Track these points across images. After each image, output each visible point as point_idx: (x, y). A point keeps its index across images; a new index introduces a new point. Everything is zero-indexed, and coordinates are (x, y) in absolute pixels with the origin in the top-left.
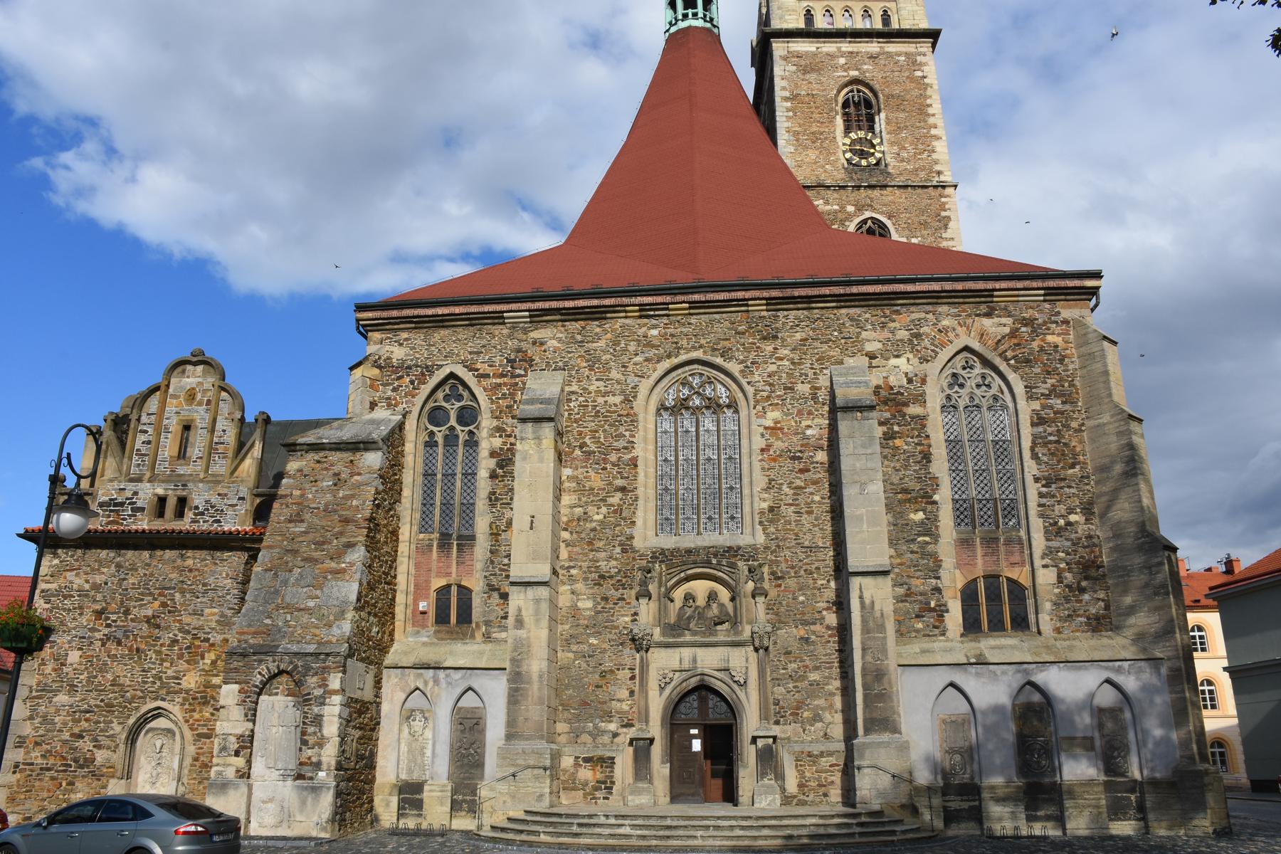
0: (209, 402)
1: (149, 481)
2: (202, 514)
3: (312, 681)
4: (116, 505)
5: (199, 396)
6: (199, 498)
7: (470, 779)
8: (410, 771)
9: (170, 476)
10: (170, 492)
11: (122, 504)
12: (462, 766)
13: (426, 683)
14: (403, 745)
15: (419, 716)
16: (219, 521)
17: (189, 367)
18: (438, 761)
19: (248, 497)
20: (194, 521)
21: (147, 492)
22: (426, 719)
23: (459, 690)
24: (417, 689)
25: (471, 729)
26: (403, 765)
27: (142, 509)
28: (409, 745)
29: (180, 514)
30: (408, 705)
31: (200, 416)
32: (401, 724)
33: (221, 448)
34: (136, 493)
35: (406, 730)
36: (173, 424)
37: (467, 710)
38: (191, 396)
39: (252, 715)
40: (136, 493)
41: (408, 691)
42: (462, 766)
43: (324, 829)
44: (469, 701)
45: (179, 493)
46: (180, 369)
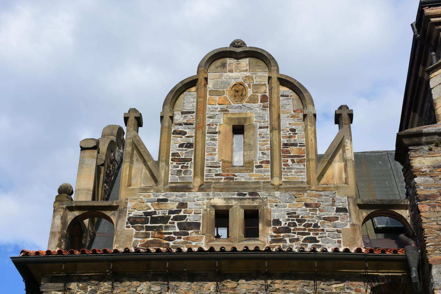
0: (264, 99)
1: (201, 189)
2: (287, 230)
4: (155, 220)
5: (250, 92)
6: (278, 208)
9: (226, 183)
10: (234, 203)
11: (164, 219)
16: (313, 240)
17: (229, 61)
19: (352, 209)
20: (275, 240)
21: (199, 205)
27: (196, 225)
29: (251, 231)
31: (255, 113)
33: (294, 151)
34: (183, 205)
36: (222, 124)
38: (239, 91)
40: (183, 205)
45: (247, 203)
46: (218, 62)
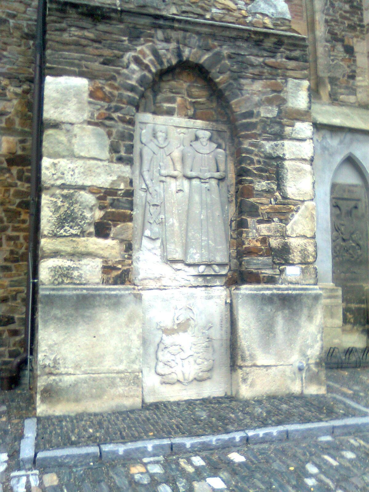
3: (254, 89)
7: (353, 280)
25: (349, 213)
39: (123, 150)
43: (313, 378)
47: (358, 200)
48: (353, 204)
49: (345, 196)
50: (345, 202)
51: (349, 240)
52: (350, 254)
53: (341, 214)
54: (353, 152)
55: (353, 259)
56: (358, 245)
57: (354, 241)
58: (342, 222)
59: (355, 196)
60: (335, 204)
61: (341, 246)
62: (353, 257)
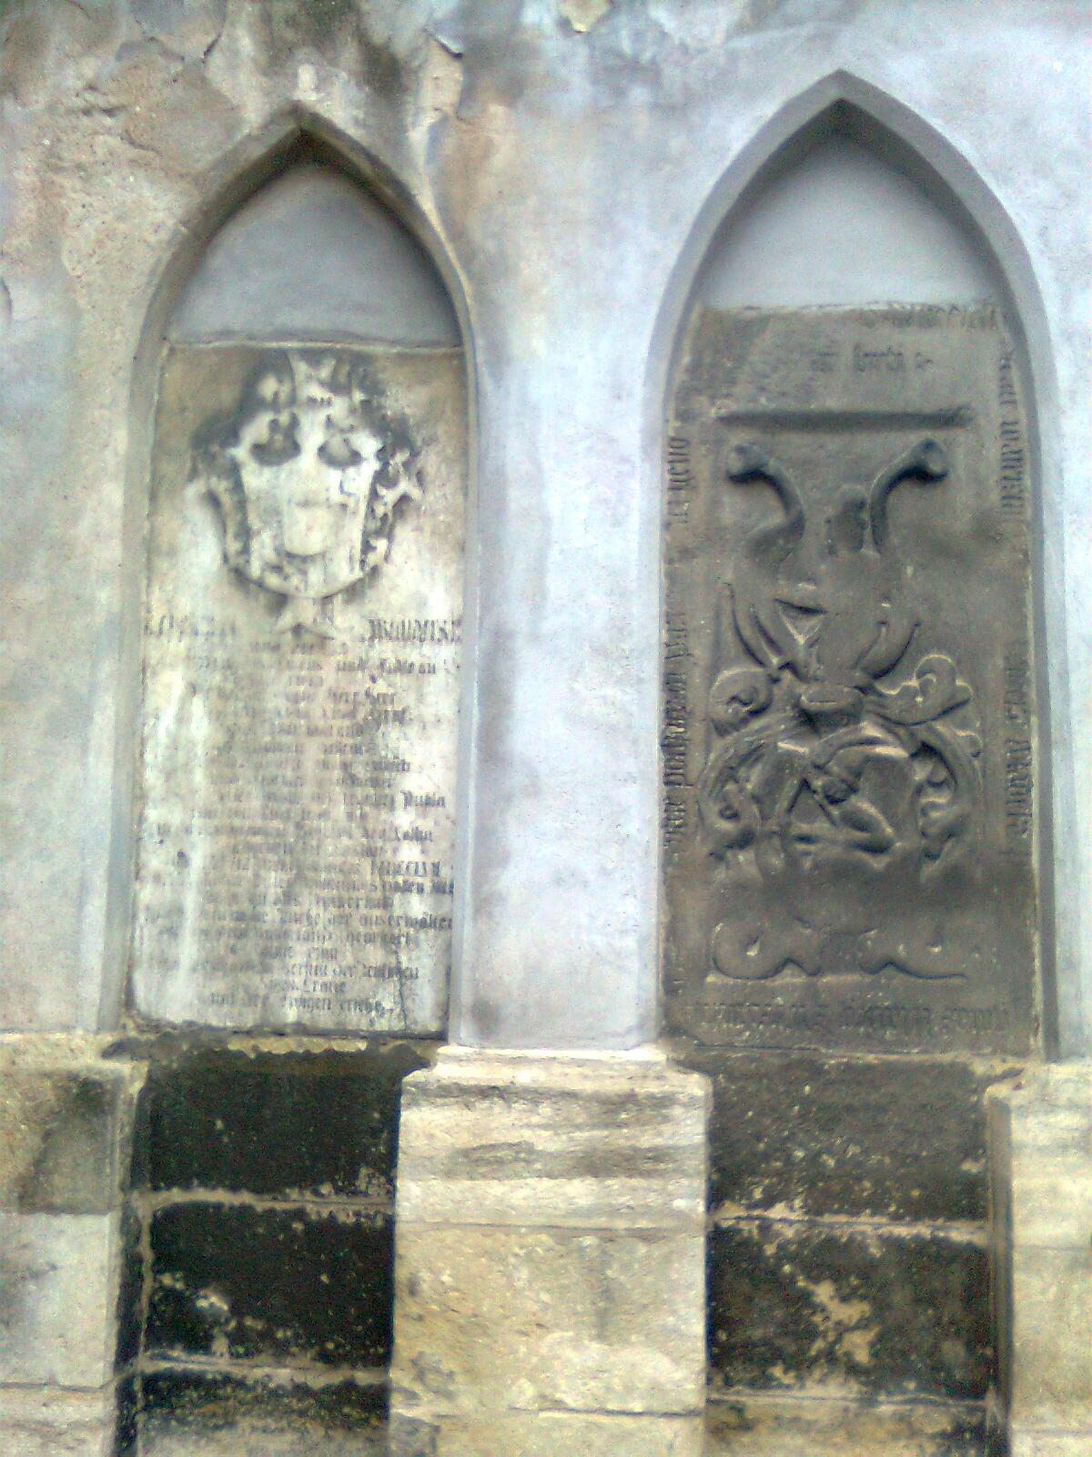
7: (873, 1019)
8: (244, 941)
12: (781, 892)
13: (386, 76)
14: (169, 686)
15: (323, 415)
18: (536, 848)
22: (396, 436)
23: (739, 129)
24: (305, 149)
25: (864, 522)
26: (181, 875)
28: (235, 693)
30: (232, 304)
32: (156, 492)
35: (202, 552)
37: (814, 340)
41: (205, 148)
42: (781, 892)
44: (847, 260)
47: (950, 419)
48: (900, 448)
49: (833, 402)
50: (833, 443)
51: (850, 716)
52: (859, 823)
53: (796, 527)
54: (865, 72)
55: (878, 863)
56: (926, 751)
57: (891, 724)
58: (804, 591)
59: (914, 394)
60: (736, 465)
61: (784, 763)
62: (877, 848)
